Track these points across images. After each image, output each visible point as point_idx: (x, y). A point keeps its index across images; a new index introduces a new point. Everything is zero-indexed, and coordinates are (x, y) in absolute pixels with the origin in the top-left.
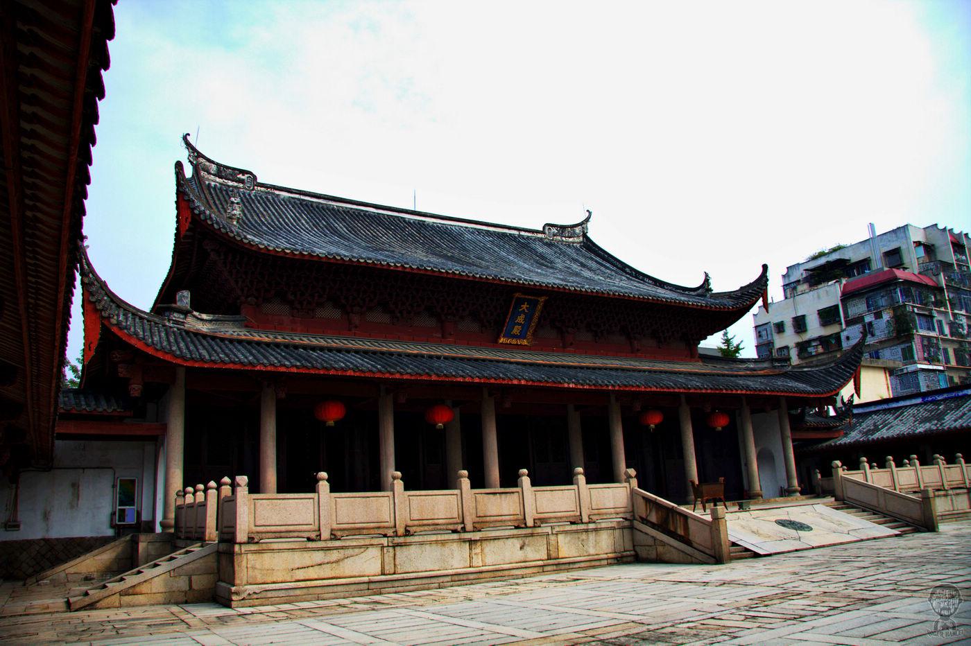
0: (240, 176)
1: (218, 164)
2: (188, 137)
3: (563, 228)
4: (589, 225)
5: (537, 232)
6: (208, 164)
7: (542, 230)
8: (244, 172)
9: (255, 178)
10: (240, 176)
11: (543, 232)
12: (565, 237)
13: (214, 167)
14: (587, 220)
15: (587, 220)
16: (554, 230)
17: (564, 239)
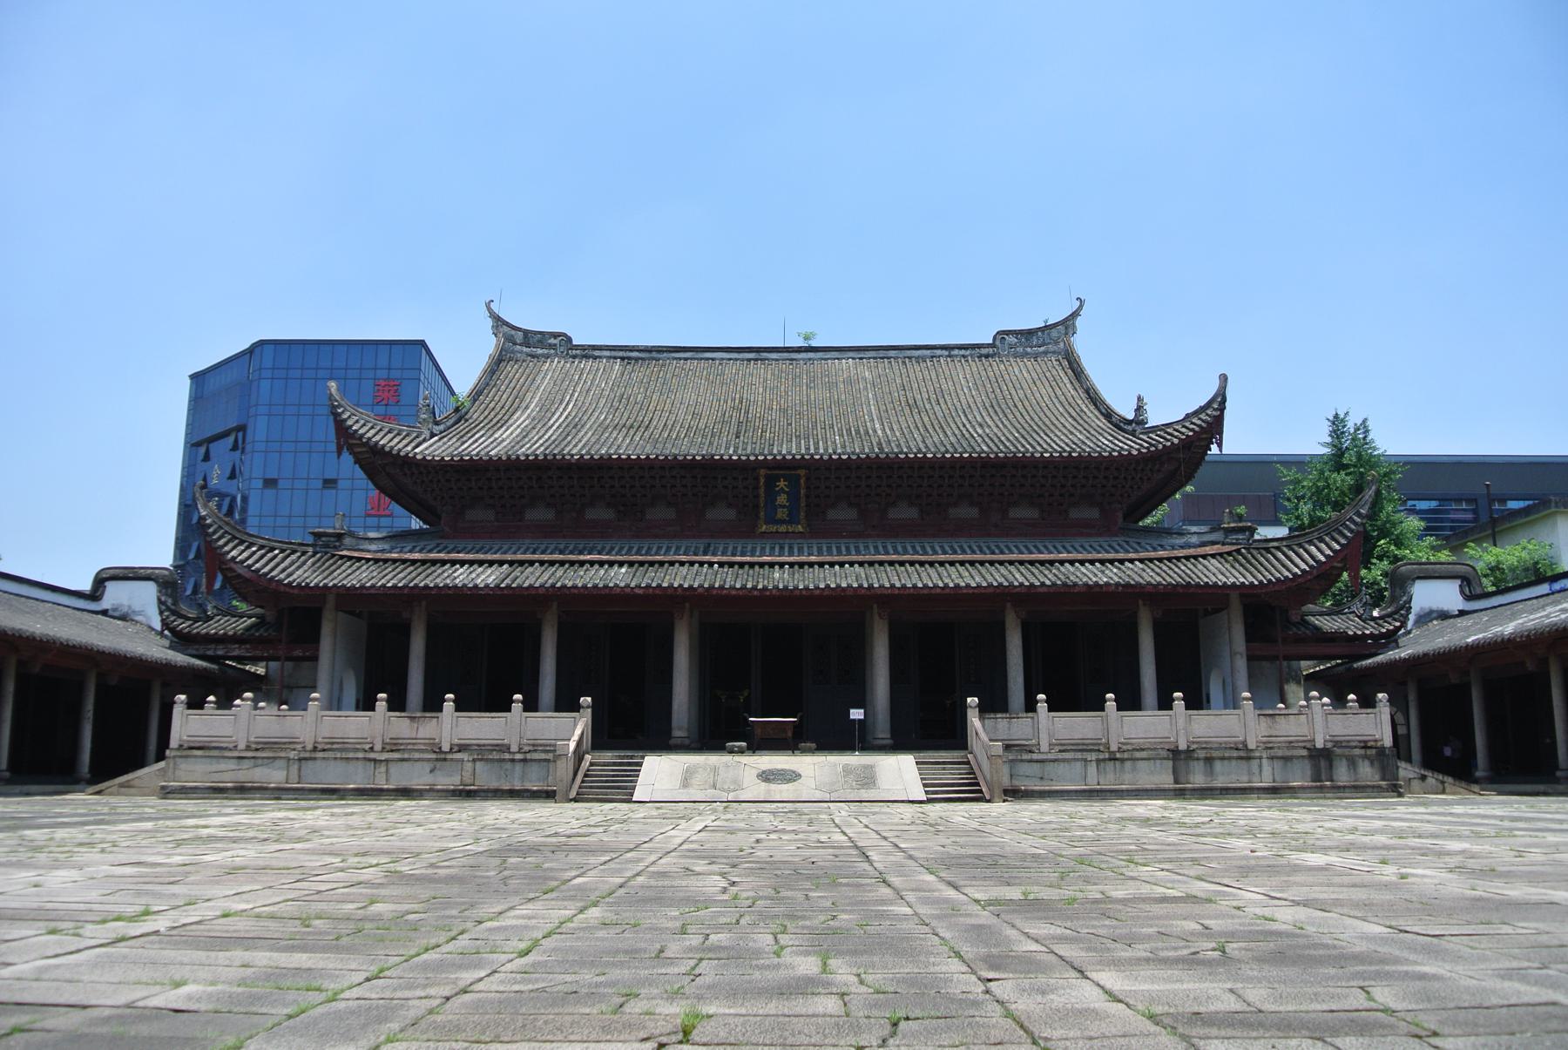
0: (552, 341)
1: (526, 333)
2: (493, 306)
3: (1030, 333)
4: (1079, 322)
5: (988, 346)
6: (513, 332)
7: (991, 342)
8: (555, 335)
9: (569, 339)
10: (552, 341)
11: (992, 345)
12: (1031, 347)
13: (519, 337)
14: (1075, 314)
15: (1075, 314)
16: (1012, 339)
17: (1029, 350)
